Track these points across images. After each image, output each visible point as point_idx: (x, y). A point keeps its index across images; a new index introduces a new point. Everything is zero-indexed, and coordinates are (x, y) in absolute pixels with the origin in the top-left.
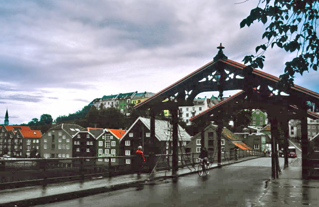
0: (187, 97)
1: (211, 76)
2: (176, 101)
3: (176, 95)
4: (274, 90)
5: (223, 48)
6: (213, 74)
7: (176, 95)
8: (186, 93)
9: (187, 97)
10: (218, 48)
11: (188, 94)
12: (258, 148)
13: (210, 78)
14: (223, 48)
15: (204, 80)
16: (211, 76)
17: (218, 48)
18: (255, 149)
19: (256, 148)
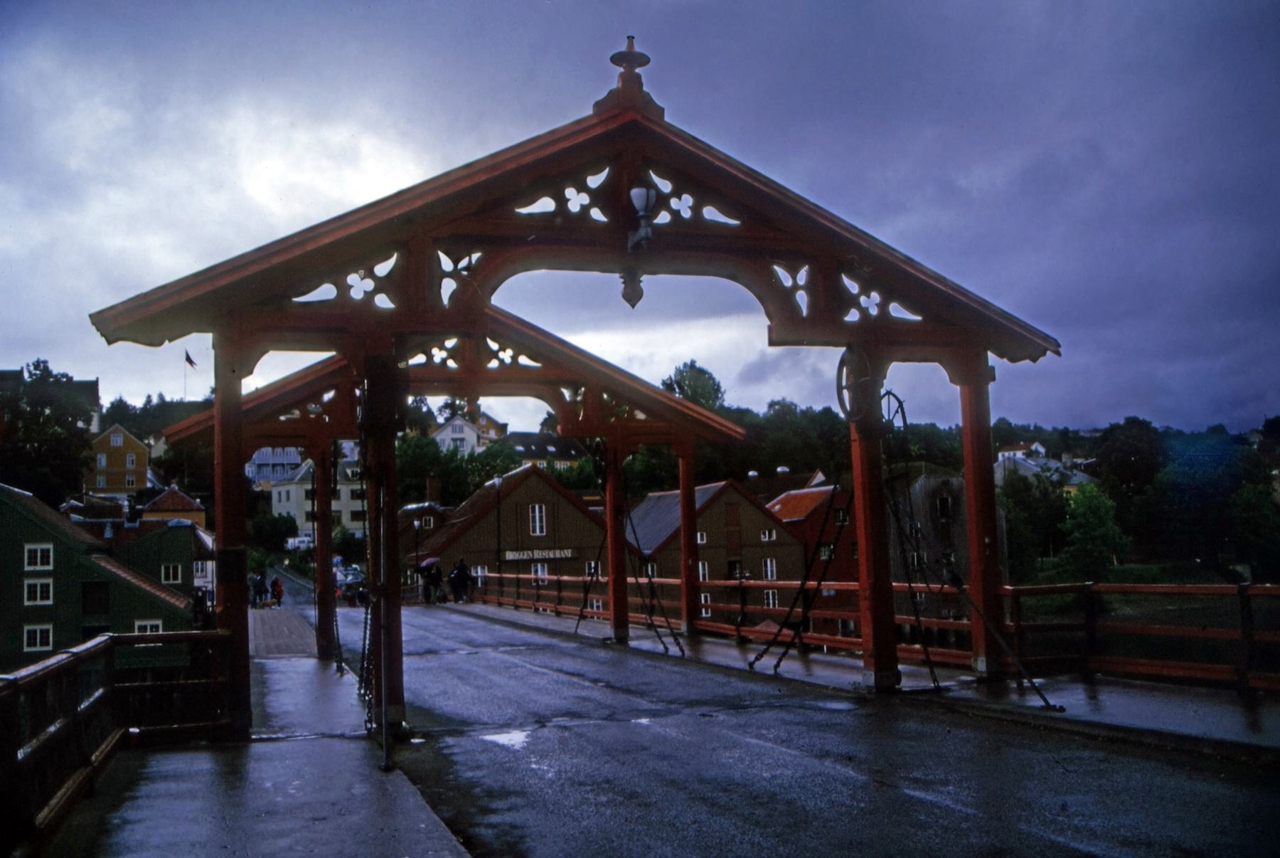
0: (448, 287)
1: (579, 192)
2: (383, 302)
3: (383, 269)
4: (865, 290)
5: (643, 60)
6: (594, 181)
7: (383, 269)
8: (446, 264)
9: (448, 287)
10: (617, 59)
11: (454, 275)
12: (175, 578)
13: (576, 200)
14: (643, 60)
15: (545, 205)
16: (579, 192)
17: (617, 59)
18: (163, 581)
19: (167, 578)
